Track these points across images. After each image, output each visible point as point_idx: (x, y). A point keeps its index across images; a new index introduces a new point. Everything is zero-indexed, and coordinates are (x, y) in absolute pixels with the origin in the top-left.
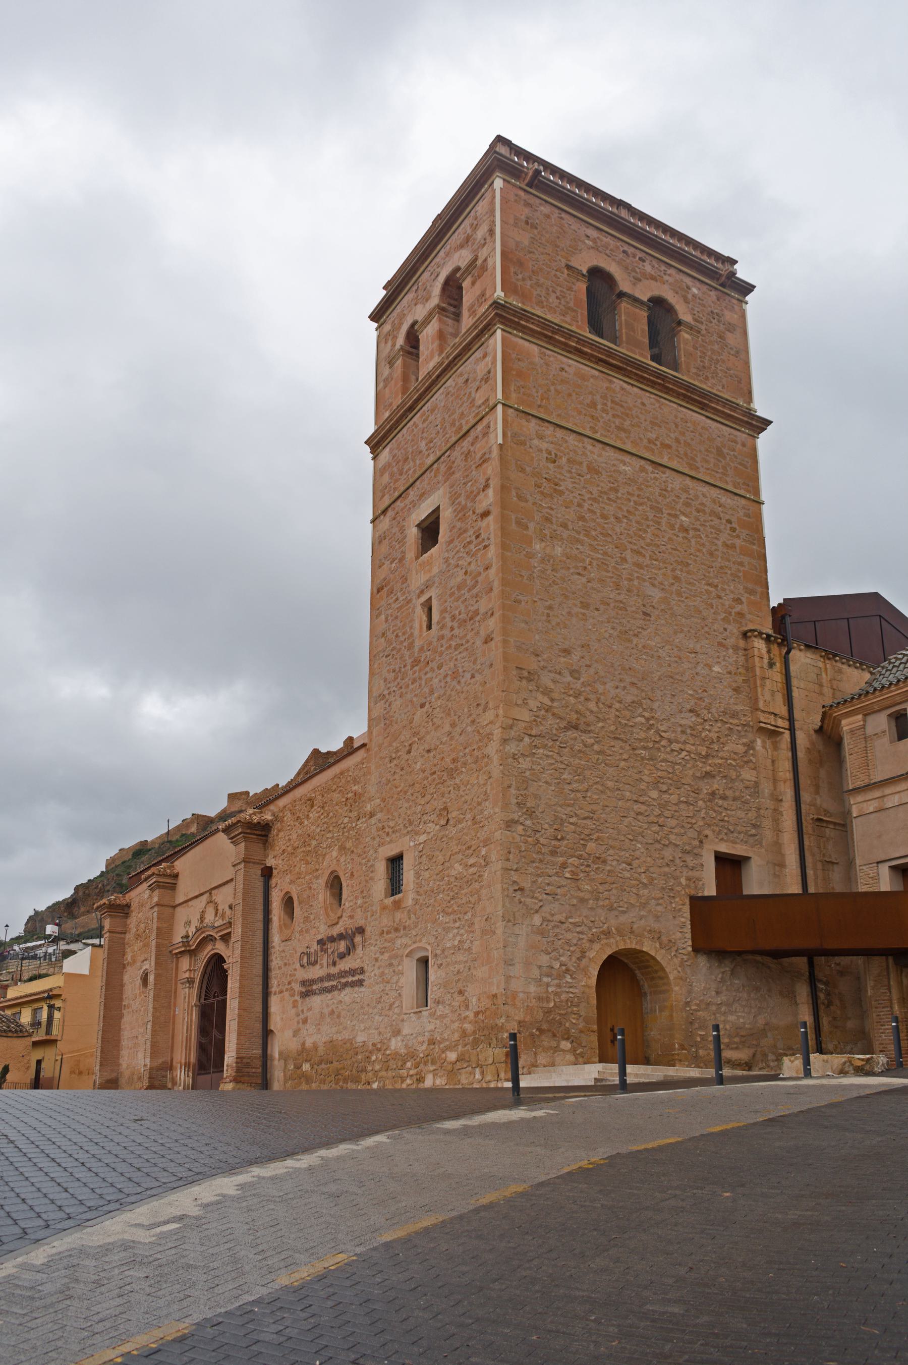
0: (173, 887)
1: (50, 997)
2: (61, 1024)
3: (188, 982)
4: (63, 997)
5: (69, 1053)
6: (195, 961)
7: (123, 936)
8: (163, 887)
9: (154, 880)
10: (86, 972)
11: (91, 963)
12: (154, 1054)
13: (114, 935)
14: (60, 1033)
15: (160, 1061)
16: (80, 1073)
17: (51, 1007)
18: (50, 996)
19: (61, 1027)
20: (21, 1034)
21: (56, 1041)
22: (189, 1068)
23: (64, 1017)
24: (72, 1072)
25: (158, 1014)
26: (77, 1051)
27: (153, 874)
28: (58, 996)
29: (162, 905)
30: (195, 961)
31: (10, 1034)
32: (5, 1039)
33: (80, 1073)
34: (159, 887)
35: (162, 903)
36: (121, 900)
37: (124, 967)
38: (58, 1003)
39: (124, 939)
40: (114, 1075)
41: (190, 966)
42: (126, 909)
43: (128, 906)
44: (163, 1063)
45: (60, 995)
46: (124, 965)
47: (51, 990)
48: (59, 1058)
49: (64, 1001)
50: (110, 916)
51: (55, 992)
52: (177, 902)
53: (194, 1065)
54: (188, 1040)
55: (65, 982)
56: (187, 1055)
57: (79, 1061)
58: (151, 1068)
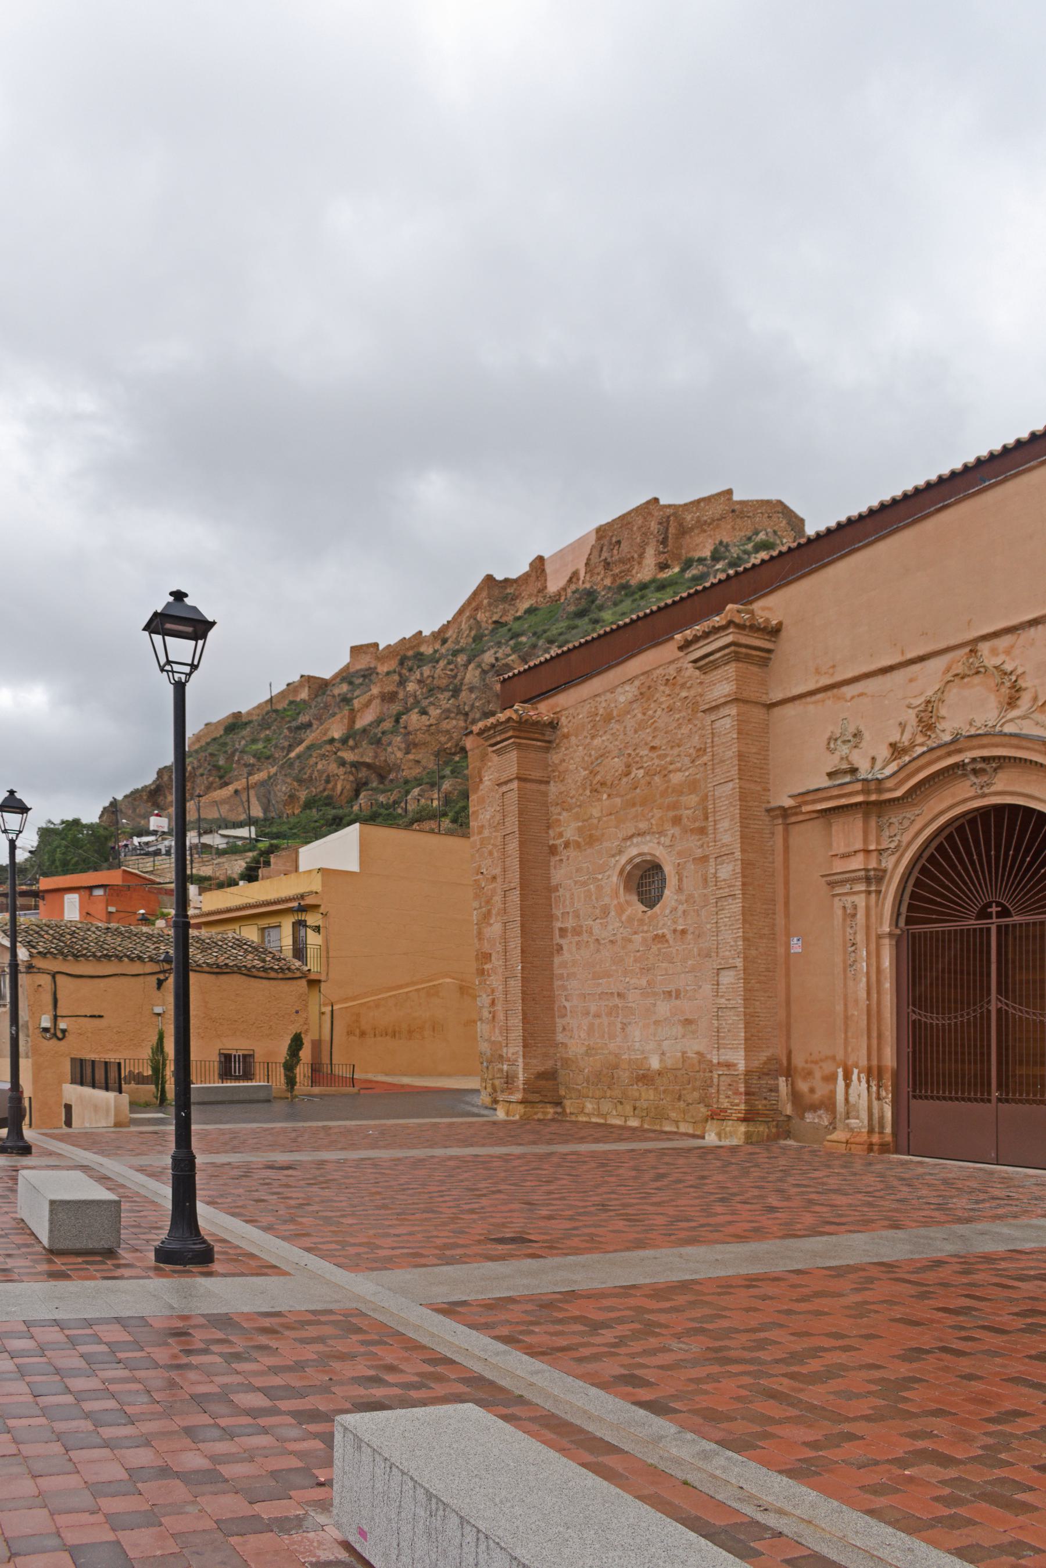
0: (763, 659)
1: (303, 909)
2: (324, 954)
3: (868, 880)
4: (322, 910)
5: (346, 1000)
6: (880, 829)
7: (543, 787)
8: (747, 659)
9: (730, 639)
10: (354, 867)
11: (361, 851)
12: (751, 1045)
13: (528, 785)
14: (324, 968)
15: (764, 1056)
16: (363, 1034)
17: (300, 924)
18: (301, 908)
19: (324, 960)
20: (290, 975)
21: (319, 981)
22: (880, 1078)
23: (326, 941)
24: (350, 1033)
25: (754, 952)
26: (354, 999)
27: (730, 623)
28: (315, 907)
29: (746, 702)
30: (880, 829)
31: (273, 974)
32: (265, 982)
33: (363, 1034)
34: (737, 658)
35: (745, 695)
36: (544, 710)
37: (553, 850)
38: (312, 919)
39: (545, 794)
40: (549, 1065)
41: (866, 840)
42: (548, 732)
43: (553, 725)
44: (770, 1060)
45: (317, 906)
46: (553, 850)
47: (302, 897)
48: (328, 1009)
49: (324, 915)
50: (519, 746)
51: (309, 901)
52: (777, 695)
53: (896, 1075)
54: (873, 1015)
55: (324, 885)
56: (874, 1050)
57: (358, 1015)
58: (748, 1073)
